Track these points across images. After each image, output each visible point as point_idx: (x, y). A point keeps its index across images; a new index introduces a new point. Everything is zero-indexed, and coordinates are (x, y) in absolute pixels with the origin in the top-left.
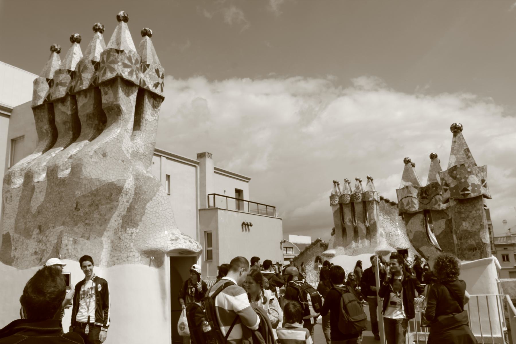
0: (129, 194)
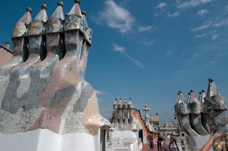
0: (78, 93)
